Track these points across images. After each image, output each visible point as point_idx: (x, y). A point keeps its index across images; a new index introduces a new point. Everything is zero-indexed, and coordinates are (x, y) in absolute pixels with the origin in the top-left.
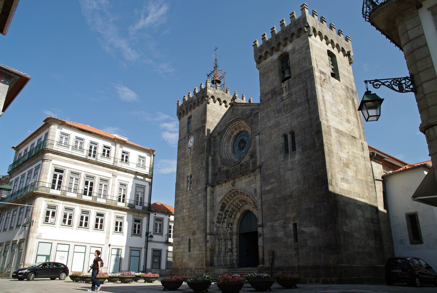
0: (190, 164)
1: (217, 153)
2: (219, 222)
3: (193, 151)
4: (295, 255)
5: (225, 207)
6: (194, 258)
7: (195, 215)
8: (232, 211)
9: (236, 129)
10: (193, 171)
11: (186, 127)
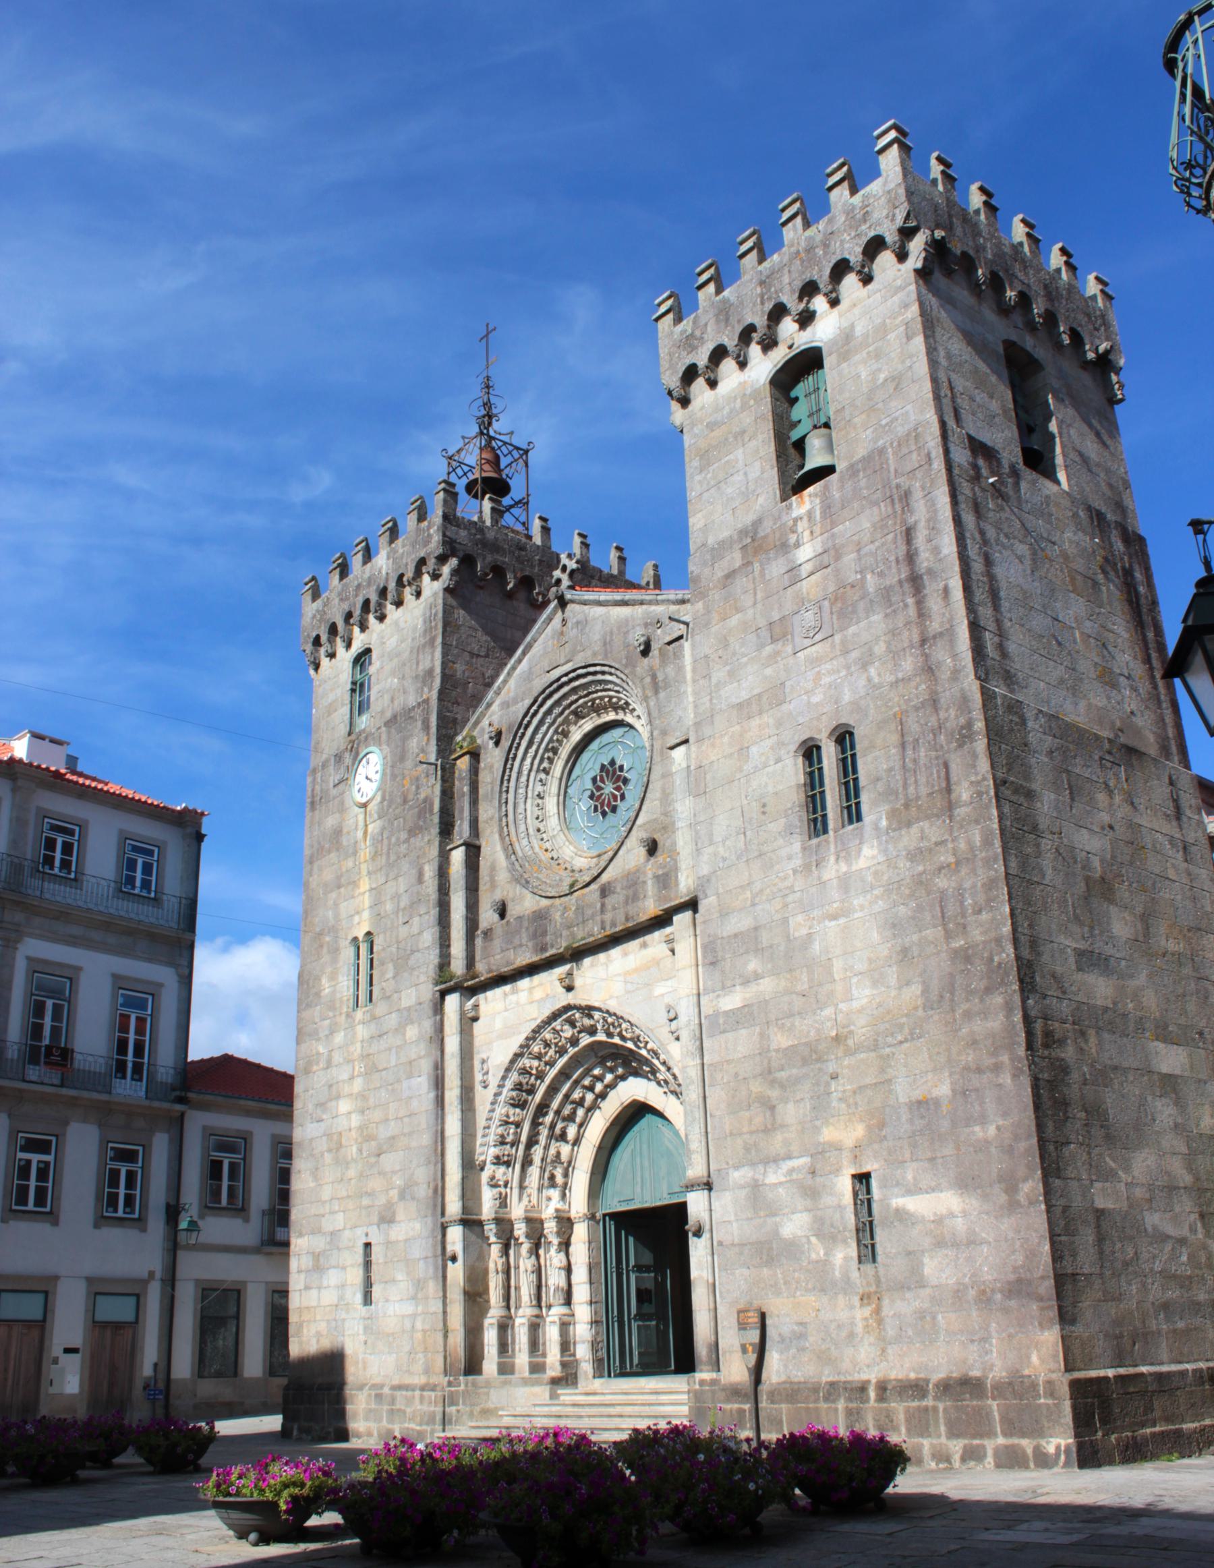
0: (365, 885)
1: (489, 831)
3: (380, 818)
4: (867, 1326)
6: (388, 1335)
7: (393, 1128)
9: (578, 715)
10: (378, 917)
11: (343, 705)
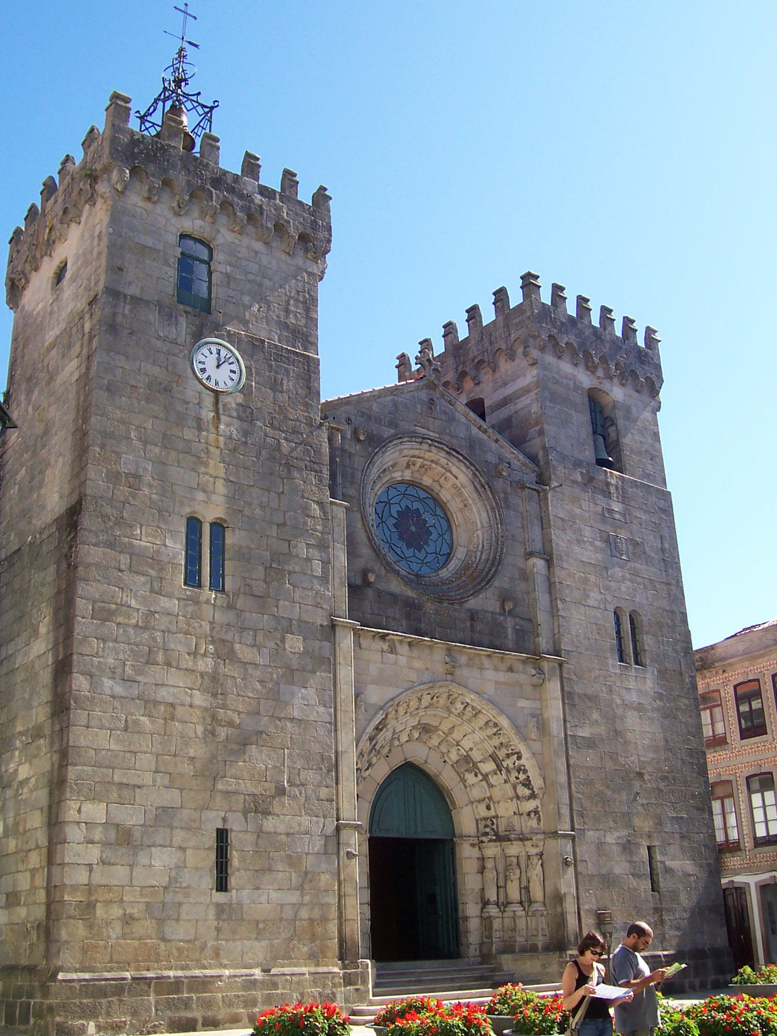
9: (408, 466)
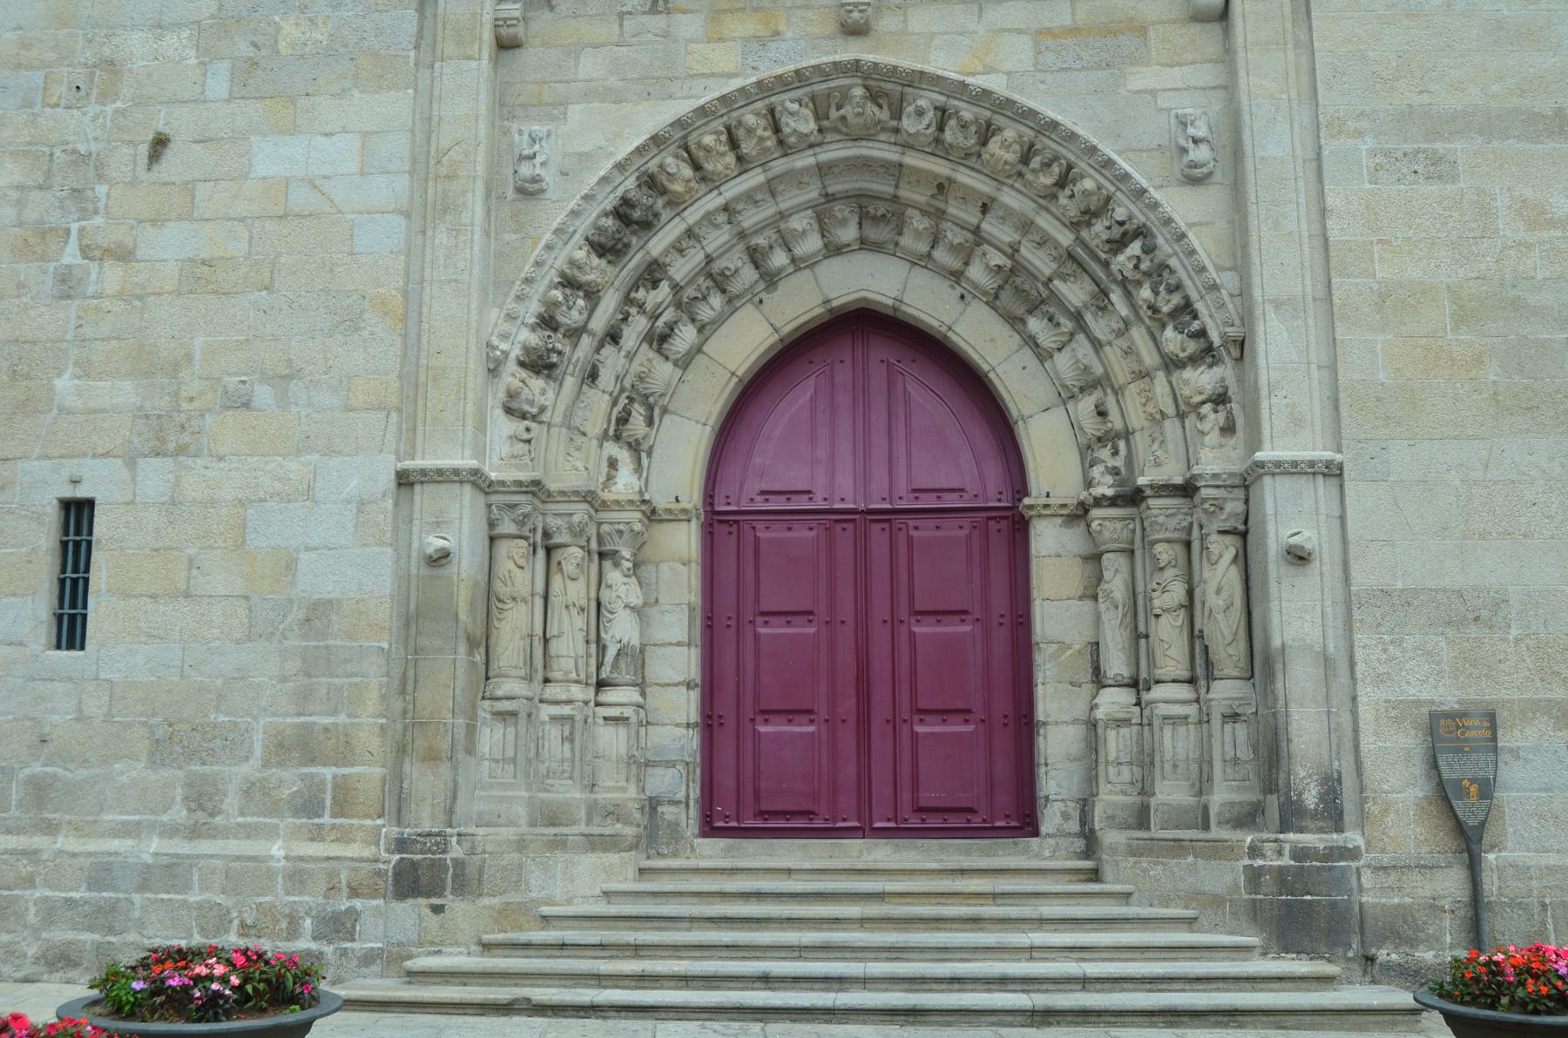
2: (552, 366)
5: (647, 225)
8: (689, 283)
